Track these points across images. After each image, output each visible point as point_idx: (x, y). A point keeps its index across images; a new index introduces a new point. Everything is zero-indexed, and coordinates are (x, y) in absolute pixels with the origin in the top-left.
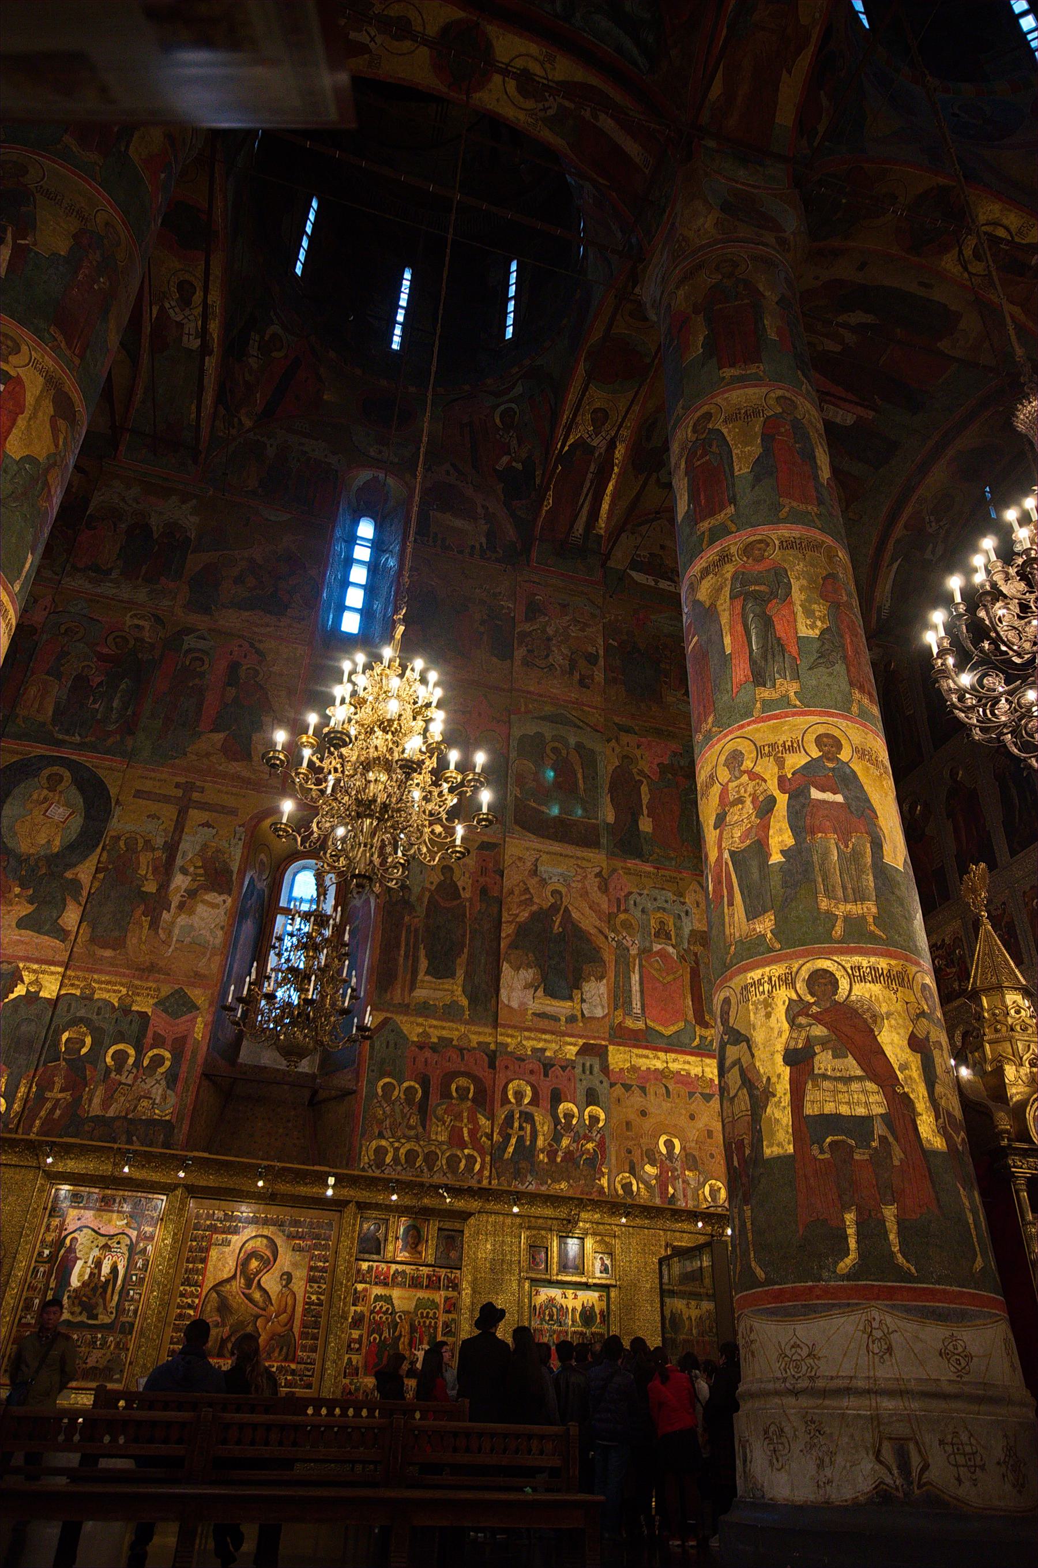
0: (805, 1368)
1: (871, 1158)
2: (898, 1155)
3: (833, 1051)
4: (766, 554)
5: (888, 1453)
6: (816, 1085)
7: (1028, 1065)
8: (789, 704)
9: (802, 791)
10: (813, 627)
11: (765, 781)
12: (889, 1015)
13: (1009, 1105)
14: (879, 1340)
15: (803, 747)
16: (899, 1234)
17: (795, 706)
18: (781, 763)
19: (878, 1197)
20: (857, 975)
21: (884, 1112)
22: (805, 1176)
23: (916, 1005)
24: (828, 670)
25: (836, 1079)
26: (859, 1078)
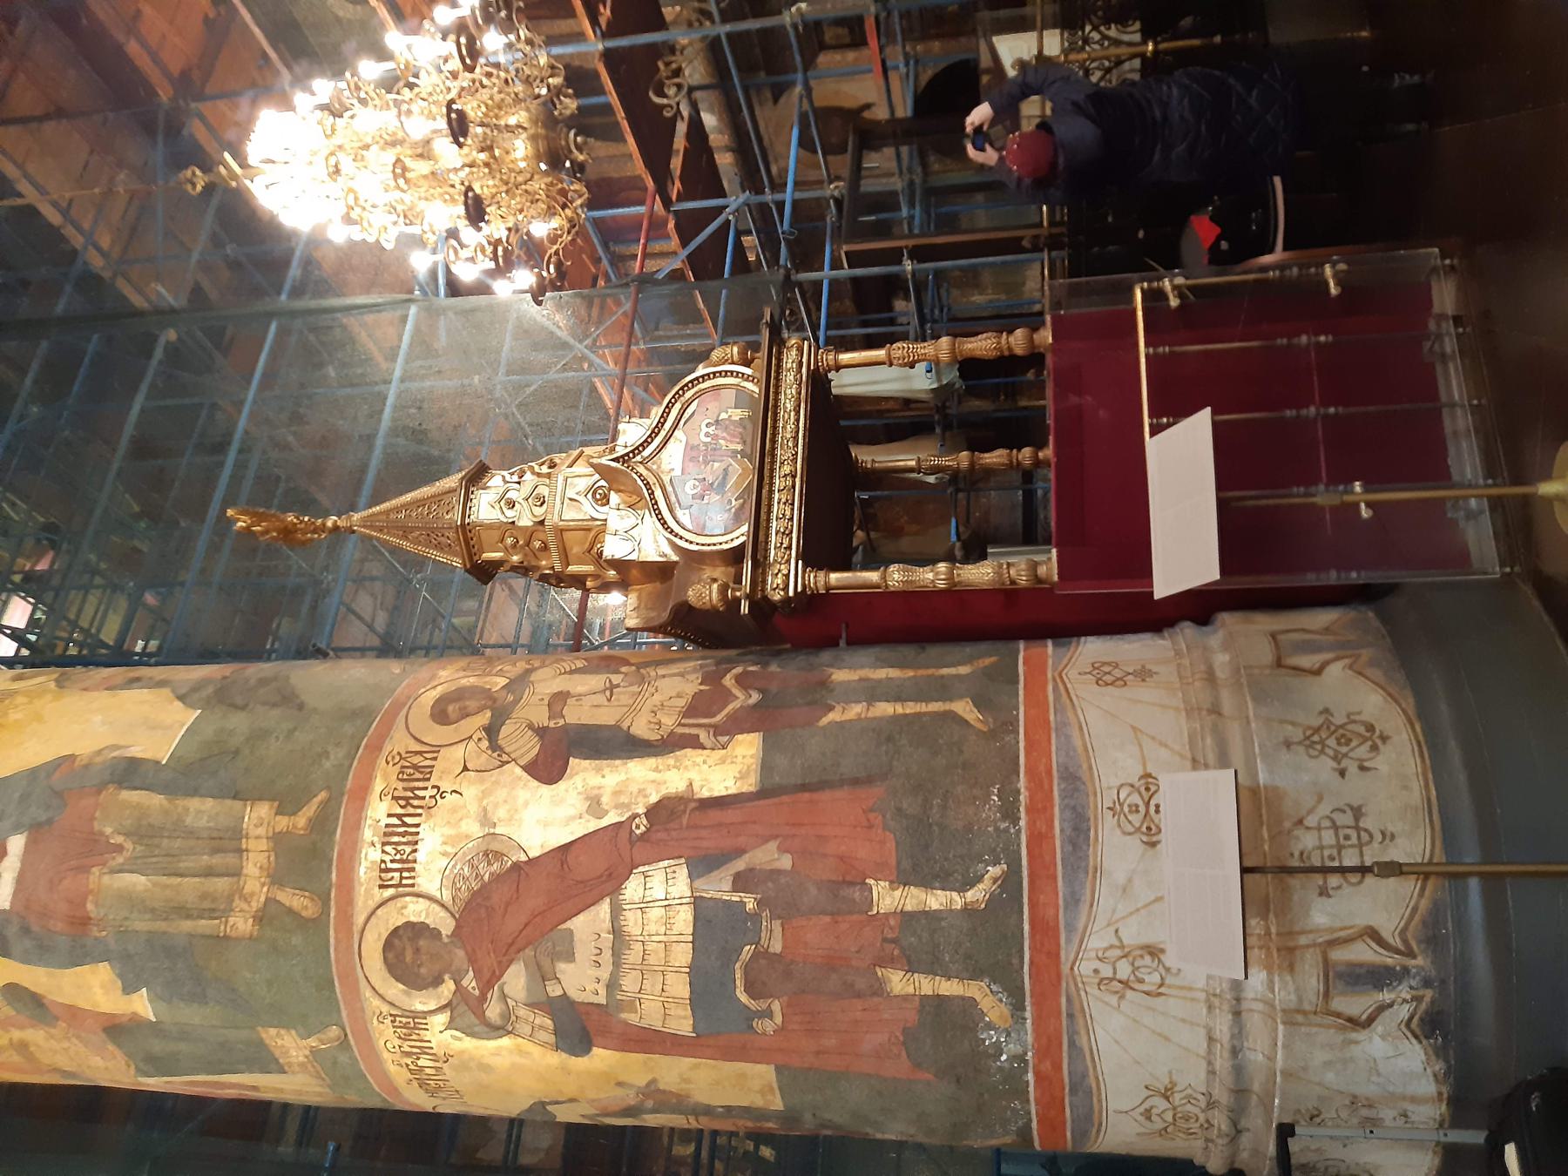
0: (1189, 1107)
1: (779, 918)
2: (769, 856)
3: (559, 960)
5: (1357, 1004)
6: (631, 1006)
12: (485, 819)
13: (676, 562)
14: (1135, 969)
16: (927, 883)
19: (855, 917)
21: (683, 872)
22: (818, 1053)
23: (472, 744)
25: (617, 963)
26: (616, 911)
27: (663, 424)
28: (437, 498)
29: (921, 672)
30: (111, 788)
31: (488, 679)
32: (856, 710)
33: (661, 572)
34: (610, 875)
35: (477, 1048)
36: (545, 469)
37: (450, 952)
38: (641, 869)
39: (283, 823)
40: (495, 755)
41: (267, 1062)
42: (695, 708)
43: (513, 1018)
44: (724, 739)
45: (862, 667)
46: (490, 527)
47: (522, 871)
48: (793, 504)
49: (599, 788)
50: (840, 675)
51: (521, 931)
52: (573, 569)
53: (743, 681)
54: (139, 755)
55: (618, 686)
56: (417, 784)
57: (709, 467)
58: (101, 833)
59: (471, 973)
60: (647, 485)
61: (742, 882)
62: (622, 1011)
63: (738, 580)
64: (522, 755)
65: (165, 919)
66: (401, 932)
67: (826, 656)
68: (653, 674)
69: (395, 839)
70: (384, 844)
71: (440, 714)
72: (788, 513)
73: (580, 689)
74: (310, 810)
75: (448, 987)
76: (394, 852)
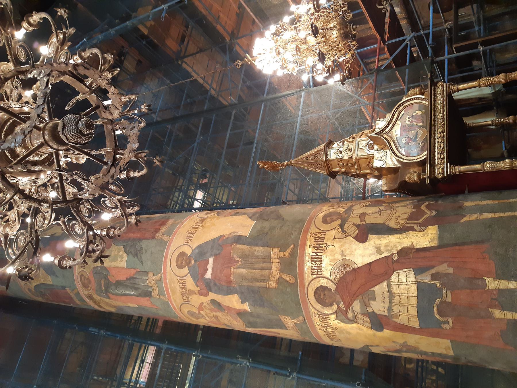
2: (444, 268)
4: (86, 276)
6: (396, 316)
7: (373, 151)
8: (160, 281)
9: (207, 283)
10: (122, 258)
11: (202, 303)
12: (343, 254)
13: (399, 167)
15: (183, 277)
17: (161, 277)
18: (192, 292)
20: (317, 271)
21: (412, 273)
23: (336, 230)
24: (144, 252)
27: (392, 120)
28: (317, 152)
29: (501, 201)
30: (234, 244)
31: (338, 209)
32: (475, 216)
33: (394, 171)
34: (386, 273)
35: (345, 326)
36: (351, 140)
37: (335, 296)
38: (397, 271)
39: (282, 254)
40: (344, 233)
41: (283, 326)
42: (412, 217)
43: (357, 318)
44: (423, 228)
45: (476, 200)
46: (334, 160)
47: (356, 271)
48: (444, 143)
49: (380, 244)
50: (467, 204)
51: (357, 290)
52: (362, 172)
53: (428, 207)
54: (241, 235)
55: (383, 210)
56: (320, 243)
57: (410, 132)
58: (233, 257)
59: (342, 303)
60: (388, 141)
61: (434, 277)
62: (393, 318)
63: (424, 171)
64: (352, 234)
65: (252, 282)
66: (319, 289)
67: (460, 197)
68: (395, 206)
69: (315, 260)
70: (312, 261)
71: (325, 220)
72: (442, 146)
73: (369, 212)
74: (289, 250)
75: (335, 307)
76: (315, 264)
